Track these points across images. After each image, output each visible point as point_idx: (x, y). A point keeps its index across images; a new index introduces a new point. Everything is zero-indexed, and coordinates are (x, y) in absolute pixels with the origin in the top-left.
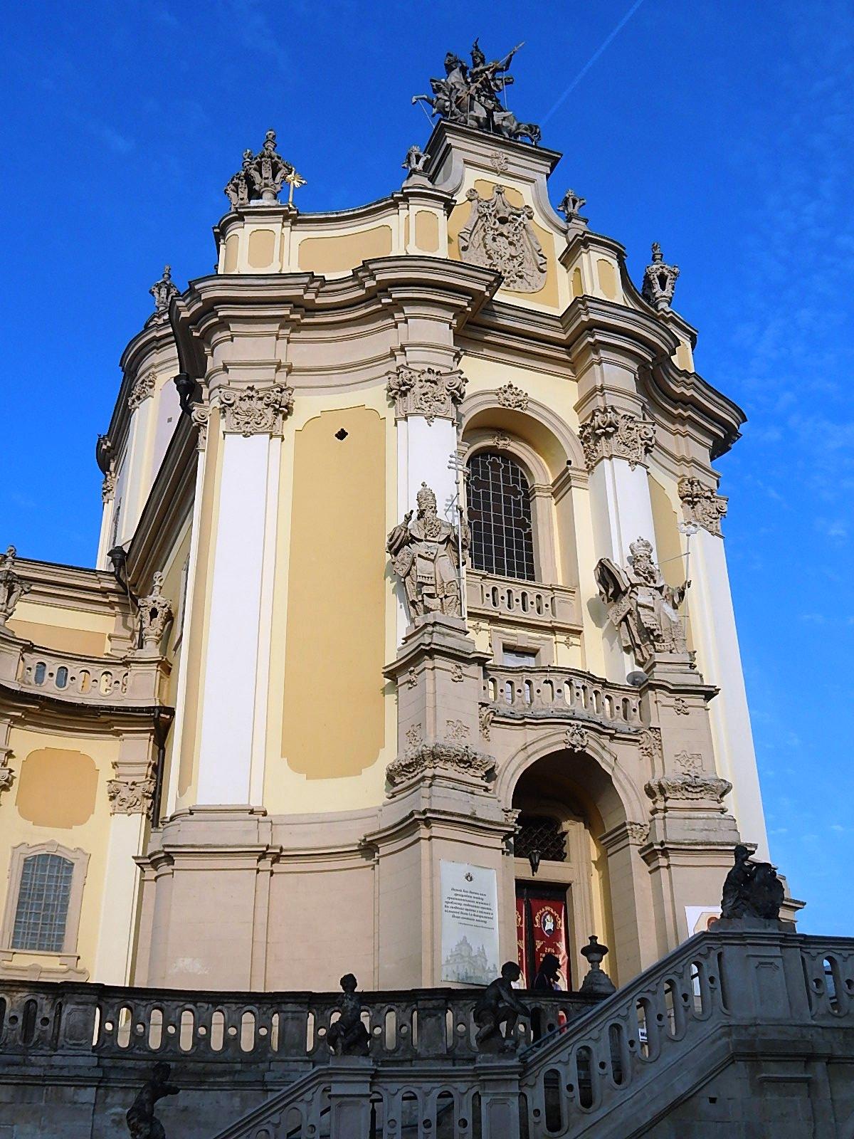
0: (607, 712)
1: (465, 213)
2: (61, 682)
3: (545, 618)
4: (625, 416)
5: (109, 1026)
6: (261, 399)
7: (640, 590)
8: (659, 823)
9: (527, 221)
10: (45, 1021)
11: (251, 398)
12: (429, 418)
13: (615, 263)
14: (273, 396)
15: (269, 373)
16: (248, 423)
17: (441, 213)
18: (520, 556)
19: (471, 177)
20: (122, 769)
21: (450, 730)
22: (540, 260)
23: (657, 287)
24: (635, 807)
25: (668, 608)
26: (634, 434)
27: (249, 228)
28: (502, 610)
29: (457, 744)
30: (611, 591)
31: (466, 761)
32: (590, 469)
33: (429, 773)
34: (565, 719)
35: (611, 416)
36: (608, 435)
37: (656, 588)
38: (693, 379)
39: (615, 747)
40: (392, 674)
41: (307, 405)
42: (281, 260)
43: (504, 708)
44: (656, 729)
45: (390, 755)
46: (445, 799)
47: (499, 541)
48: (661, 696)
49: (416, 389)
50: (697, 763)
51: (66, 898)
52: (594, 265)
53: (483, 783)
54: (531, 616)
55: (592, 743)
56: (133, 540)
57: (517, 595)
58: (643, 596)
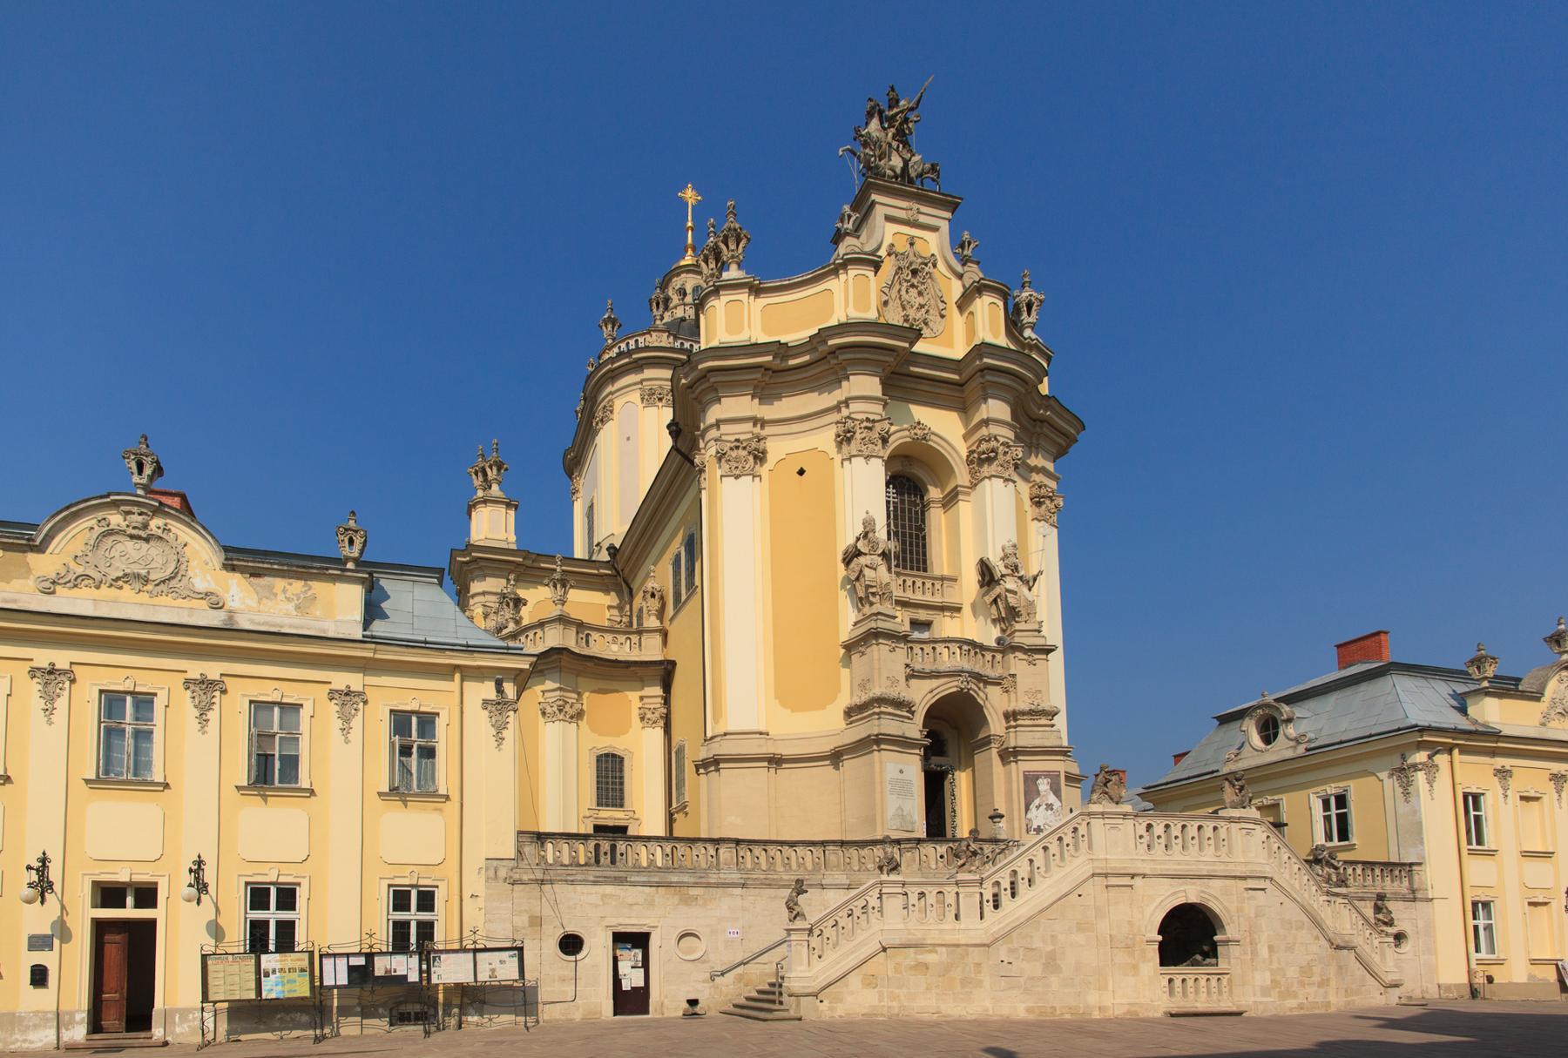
7: (1008, 579)
12: (867, 458)
25: (1025, 590)
26: (1008, 457)
29: (892, 693)
31: (898, 704)
34: (956, 673)
35: (993, 444)
36: (990, 460)
37: (1021, 578)
38: (1052, 402)
39: (990, 689)
40: (849, 647)
43: (918, 667)
48: (1020, 655)
49: (858, 436)
58: (1010, 583)
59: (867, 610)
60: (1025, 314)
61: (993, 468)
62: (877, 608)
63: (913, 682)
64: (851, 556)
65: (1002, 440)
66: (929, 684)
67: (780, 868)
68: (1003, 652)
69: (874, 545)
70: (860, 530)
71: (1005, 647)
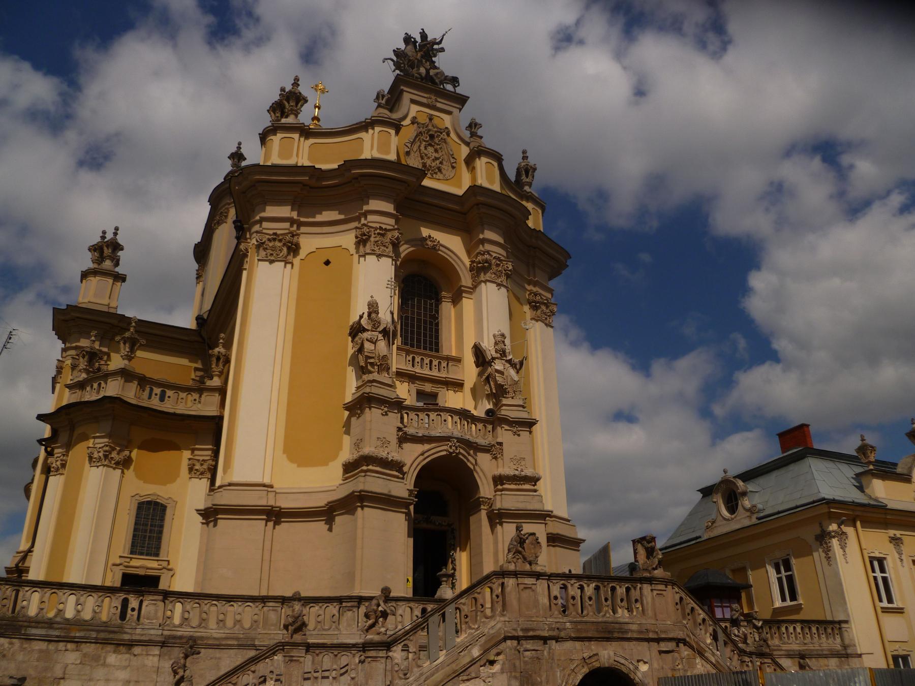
0: (474, 433)
1: (409, 132)
2: (162, 399)
3: (443, 374)
4: (495, 258)
5: (169, 613)
6: (280, 241)
7: (497, 361)
8: (498, 498)
9: (446, 137)
10: (133, 610)
11: (274, 240)
12: (379, 256)
13: (496, 164)
14: (288, 238)
15: (287, 225)
16: (272, 255)
17: (393, 132)
18: (431, 337)
19: (415, 109)
20: (196, 452)
21: (379, 443)
22: (452, 161)
23: (524, 177)
24: (486, 489)
25: (512, 372)
27: (280, 135)
28: (418, 370)
29: (382, 453)
30: (481, 360)
32: (475, 287)
33: (364, 468)
34: (447, 439)
35: (487, 256)
41: (309, 243)
42: (297, 156)
43: (411, 431)
44: (501, 444)
45: (346, 454)
46: (374, 483)
47: (419, 327)
49: (372, 239)
50: (523, 463)
51: (162, 526)
52: (484, 165)
53: (397, 474)
54: (435, 373)
55: (462, 451)
56: (210, 311)
57: (427, 361)
58: (498, 365)
59: (366, 377)
60: (524, 177)
61: (489, 276)
62: (375, 376)
63: (405, 445)
64: (356, 330)
65: (494, 255)
66: (420, 448)
67: (212, 624)
68: (492, 423)
69: (376, 323)
70: (366, 311)
71: (493, 419)
